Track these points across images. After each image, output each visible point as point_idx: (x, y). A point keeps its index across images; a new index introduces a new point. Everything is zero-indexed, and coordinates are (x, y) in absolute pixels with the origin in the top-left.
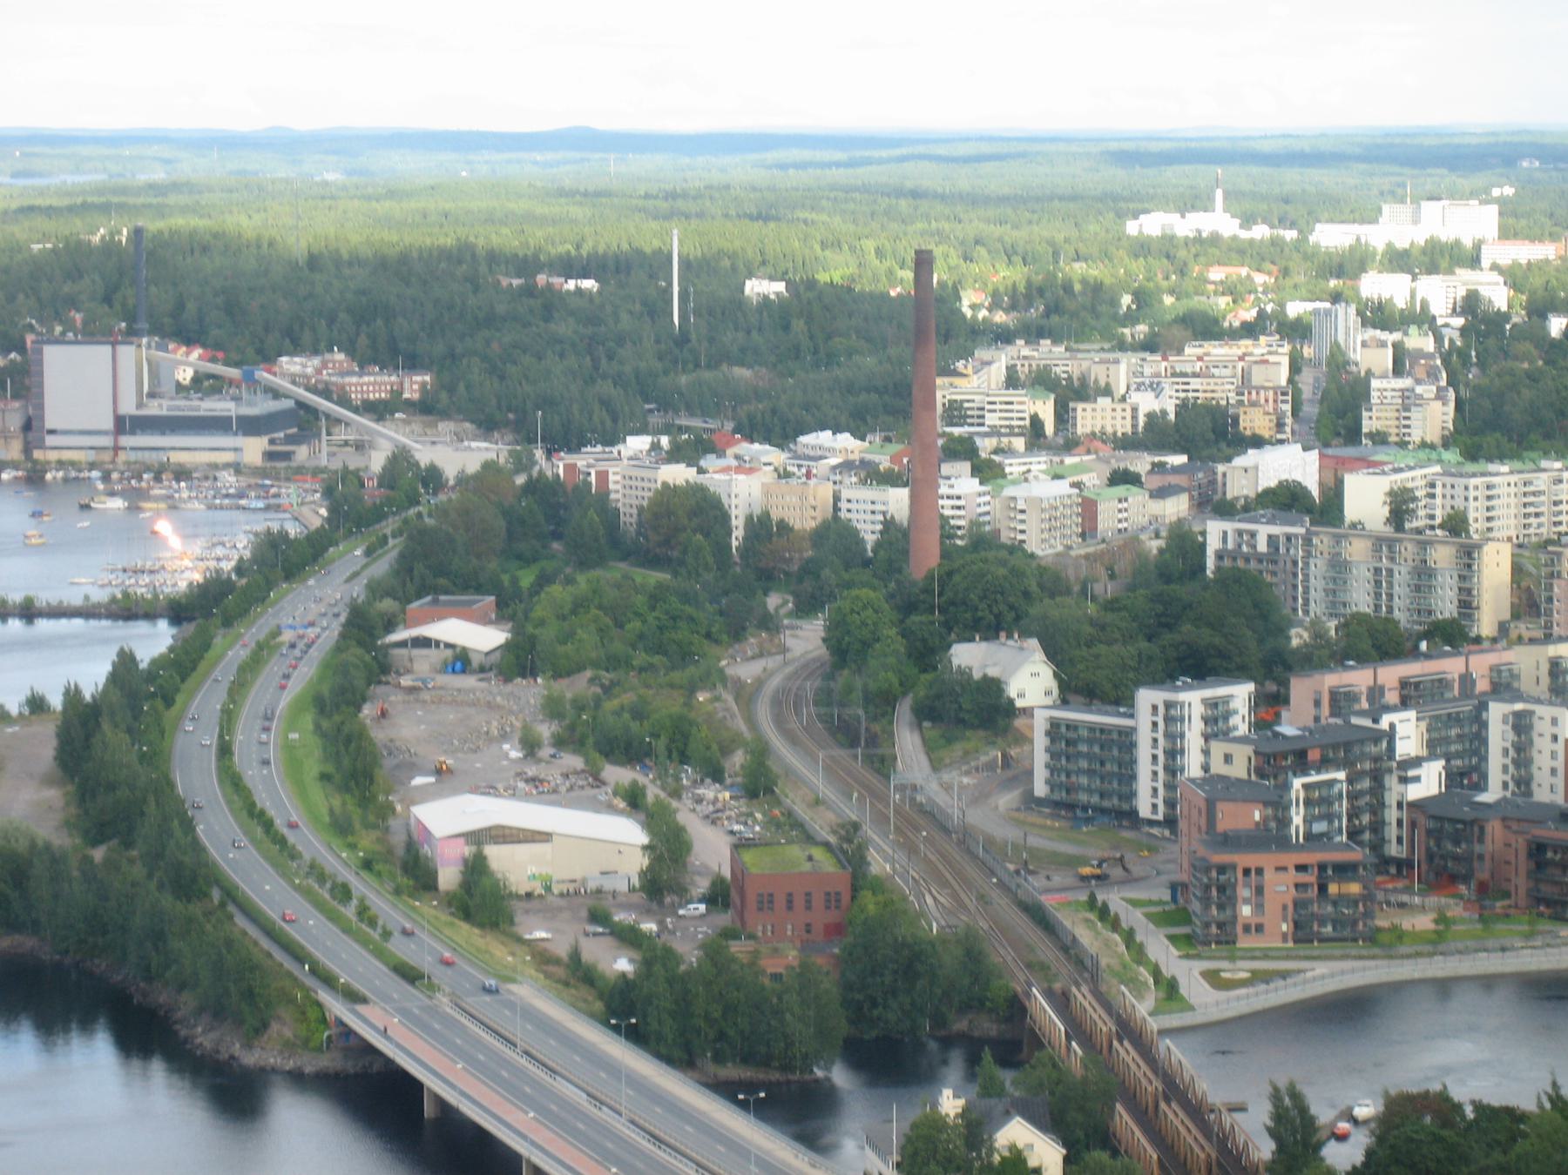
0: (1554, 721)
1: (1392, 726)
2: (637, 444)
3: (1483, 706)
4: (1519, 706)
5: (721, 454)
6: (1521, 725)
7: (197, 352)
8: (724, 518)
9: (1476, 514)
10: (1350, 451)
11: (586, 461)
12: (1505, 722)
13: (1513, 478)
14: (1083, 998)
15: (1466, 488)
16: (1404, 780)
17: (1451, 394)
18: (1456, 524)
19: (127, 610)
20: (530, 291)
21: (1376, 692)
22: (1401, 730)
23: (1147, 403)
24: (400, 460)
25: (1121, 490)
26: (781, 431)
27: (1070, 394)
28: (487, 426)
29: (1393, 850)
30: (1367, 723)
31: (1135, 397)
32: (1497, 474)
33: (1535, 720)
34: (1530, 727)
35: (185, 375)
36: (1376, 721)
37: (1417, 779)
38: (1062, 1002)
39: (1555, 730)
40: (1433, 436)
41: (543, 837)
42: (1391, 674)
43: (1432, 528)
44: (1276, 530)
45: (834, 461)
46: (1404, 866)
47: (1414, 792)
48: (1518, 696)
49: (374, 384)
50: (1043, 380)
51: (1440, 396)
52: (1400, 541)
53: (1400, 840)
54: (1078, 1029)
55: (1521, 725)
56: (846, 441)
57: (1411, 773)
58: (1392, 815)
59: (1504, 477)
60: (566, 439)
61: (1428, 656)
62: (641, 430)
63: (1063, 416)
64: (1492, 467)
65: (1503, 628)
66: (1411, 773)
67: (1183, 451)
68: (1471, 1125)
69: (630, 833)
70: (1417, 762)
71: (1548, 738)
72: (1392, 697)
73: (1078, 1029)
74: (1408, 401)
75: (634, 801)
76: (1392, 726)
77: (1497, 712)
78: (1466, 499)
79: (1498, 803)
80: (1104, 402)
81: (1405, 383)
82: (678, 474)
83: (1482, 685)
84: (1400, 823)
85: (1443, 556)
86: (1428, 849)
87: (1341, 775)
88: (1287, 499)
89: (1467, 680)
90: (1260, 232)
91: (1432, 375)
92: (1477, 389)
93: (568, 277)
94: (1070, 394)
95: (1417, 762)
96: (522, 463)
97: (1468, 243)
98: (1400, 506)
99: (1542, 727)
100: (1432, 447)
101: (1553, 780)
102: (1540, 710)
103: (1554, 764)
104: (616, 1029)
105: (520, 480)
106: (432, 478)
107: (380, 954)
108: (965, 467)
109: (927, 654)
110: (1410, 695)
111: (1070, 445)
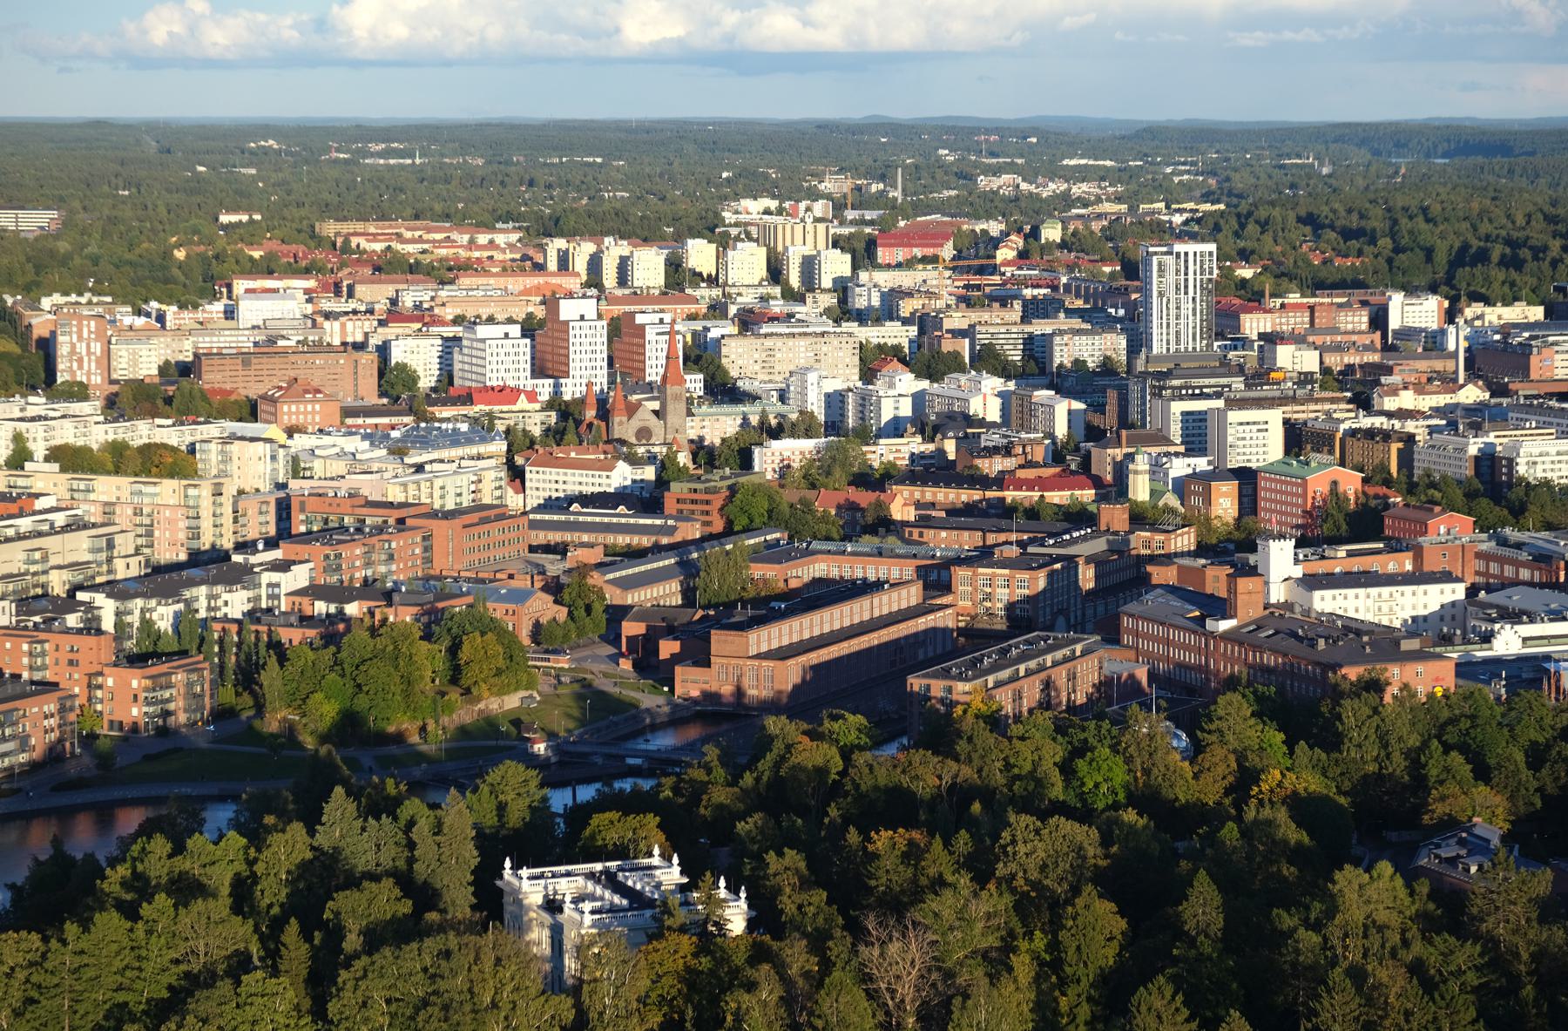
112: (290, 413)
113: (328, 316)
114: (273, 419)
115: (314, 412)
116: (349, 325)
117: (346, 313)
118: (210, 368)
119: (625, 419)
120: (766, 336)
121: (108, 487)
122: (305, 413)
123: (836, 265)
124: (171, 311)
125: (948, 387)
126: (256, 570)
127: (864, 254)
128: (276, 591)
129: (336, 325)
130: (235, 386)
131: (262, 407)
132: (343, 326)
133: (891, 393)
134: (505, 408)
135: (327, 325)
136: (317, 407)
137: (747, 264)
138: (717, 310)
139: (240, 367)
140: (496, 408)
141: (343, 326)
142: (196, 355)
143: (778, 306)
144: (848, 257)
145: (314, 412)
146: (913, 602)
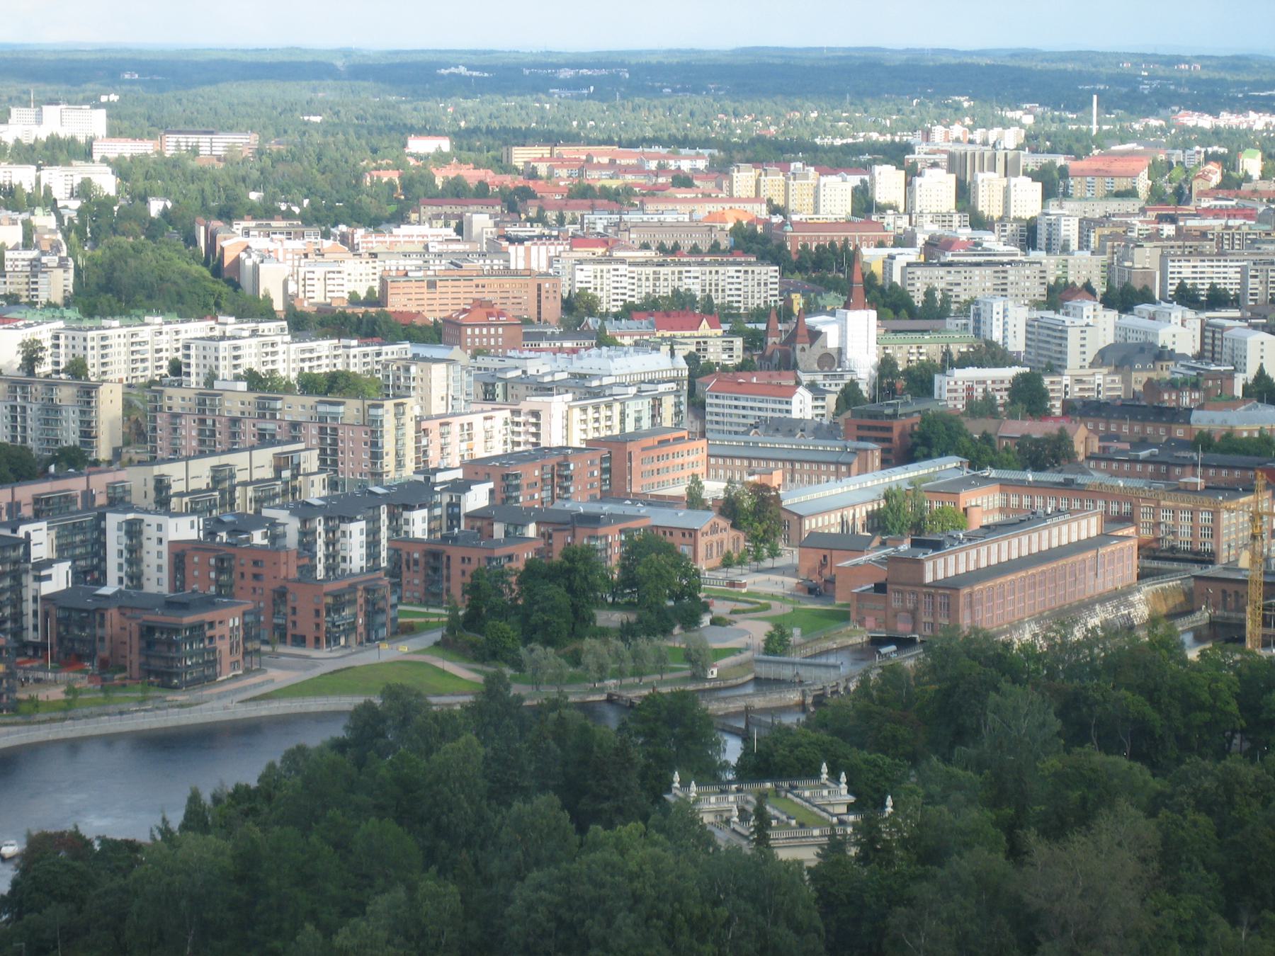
0: (160, 527)
1: (28, 535)
3: (102, 517)
4: (131, 516)
6: (133, 531)
9: (93, 360)
12: (119, 529)
13: (124, 331)
15: (85, 340)
16: (39, 579)
17: (71, 263)
18: (77, 369)
21: (14, 507)
22: (35, 538)
29: (30, 636)
30: (7, 532)
32: (109, 328)
33: (144, 527)
34: (140, 532)
36: (14, 531)
37: (49, 577)
39: (160, 534)
40: (57, 298)
42: (26, 493)
43: (57, 372)
46: (39, 648)
47: (47, 588)
48: (130, 508)
51: (62, 264)
52: (31, 383)
53: (35, 628)
55: (133, 531)
57: (44, 573)
58: (29, 607)
59: (116, 331)
61: (56, 477)
64: (105, 322)
65: (117, 453)
66: (44, 573)
68: (98, 856)
70: (49, 563)
71: (155, 541)
72: (27, 511)
74: (36, 267)
76: (28, 535)
77: (113, 521)
78: (85, 348)
79: (115, 594)
81: (33, 254)
83: (101, 500)
84: (35, 613)
85: (66, 395)
86: (59, 634)
89: (88, 496)
91: (55, 248)
92: (91, 259)
95: (49, 563)
97: (82, 139)
99: (150, 532)
100: (55, 306)
101: (159, 575)
102: (148, 518)
103: (160, 562)
110: (43, 508)
112: (473, 336)
113: (512, 240)
114: (457, 340)
115: (496, 336)
116: (534, 249)
117: (530, 238)
118: (396, 291)
119: (806, 346)
120: (950, 264)
122: (489, 336)
124: (360, 233)
125: (1136, 321)
126: (437, 489)
128: (456, 510)
129: (521, 249)
130: (420, 309)
131: (447, 330)
132: (528, 250)
133: (1078, 322)
134: (687, 333)
135: (512, 249)
136: (500, 330)
138: (904, 240)
139: (425, 290)
140: (678, 333)
141: (528, 250)
142: (383, 281)
143: (965, 233)
144: (1039, 185)
145: (496, 336)
146: (1093, 533)
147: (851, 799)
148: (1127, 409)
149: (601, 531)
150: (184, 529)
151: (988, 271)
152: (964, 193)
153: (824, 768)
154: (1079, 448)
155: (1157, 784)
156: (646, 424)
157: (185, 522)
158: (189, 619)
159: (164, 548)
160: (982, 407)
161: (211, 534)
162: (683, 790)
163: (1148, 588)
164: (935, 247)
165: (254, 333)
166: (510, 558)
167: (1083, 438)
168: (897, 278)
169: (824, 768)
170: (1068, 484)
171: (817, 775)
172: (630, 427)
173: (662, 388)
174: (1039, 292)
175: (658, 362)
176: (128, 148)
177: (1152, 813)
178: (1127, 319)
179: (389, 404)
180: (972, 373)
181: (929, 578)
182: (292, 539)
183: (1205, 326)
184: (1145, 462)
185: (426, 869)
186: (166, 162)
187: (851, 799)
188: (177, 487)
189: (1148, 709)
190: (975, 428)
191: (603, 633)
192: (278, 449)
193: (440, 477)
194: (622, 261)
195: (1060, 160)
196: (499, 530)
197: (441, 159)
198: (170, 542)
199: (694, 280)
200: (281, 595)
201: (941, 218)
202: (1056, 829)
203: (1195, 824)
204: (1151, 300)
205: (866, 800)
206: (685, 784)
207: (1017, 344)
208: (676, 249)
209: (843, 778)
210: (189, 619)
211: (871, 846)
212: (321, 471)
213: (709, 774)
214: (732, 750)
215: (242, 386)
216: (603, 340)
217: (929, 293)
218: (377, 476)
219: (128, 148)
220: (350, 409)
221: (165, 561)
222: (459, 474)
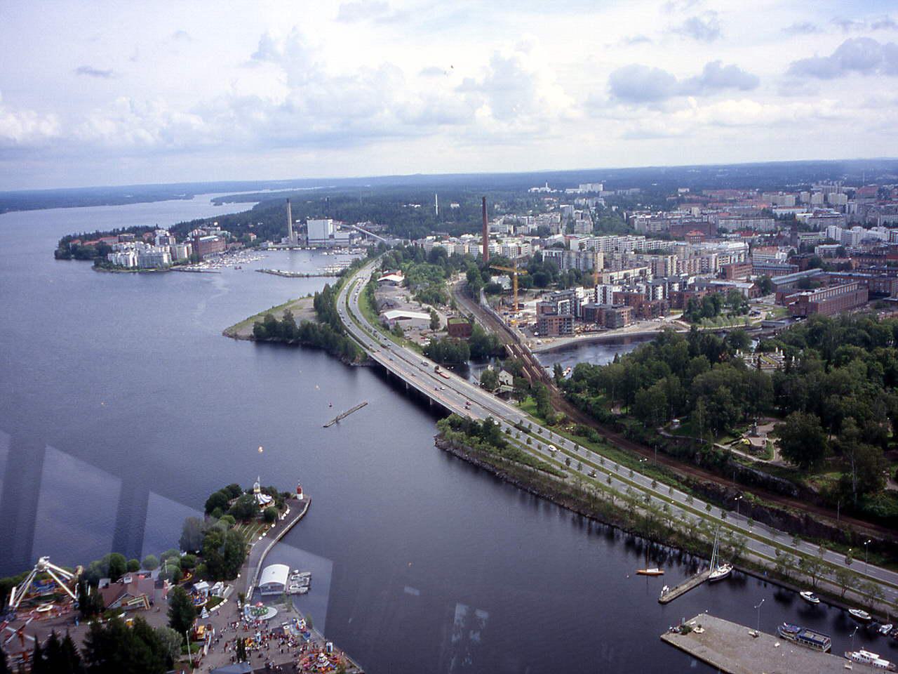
2: (429, 238)
5: (446, 240)
6: (605, 290)
7: (341, 223)
8: (446, 253)
10: (572, 235)
11: (419, 242)
14: (516, 346)
17: (592, 223)
18: (592, 249)
19: (328, 275)
20: (407, 208)
23: (531, 226)
24: (381, 244)
25: (525, 245)
26: (458, 235)
27: (517, 224)
28: (400, 236)
31: (529, 225)
35: (339, 227)
38: (513, 347)
41: (410, 318)
44: (556, 252)
45: (469, 240)
47: (583, 304)
49: (377, 227)
50: (510, 222)
54: (516, 352)
55: (605, 290)
56: (471, 236)
59: (602, 239)
60: (415, 238)
62: (431, 235)
63: (515, 230)
65: (602, 270)
67: (538, 236)
68: (592, 369)
69: (427, 317)
73: (516, 352)
75: (428, 311)
80: (523, 227)
82: (437, 244)
85: (590, 256)
87: (568, 300)
88: (558, 245)
90: (555, 191)
92: (598, 222)
93: (415, 204)
94: (517, 224)
96: (406, 243)
98: (581, 246)
104: (424, 356)
105: (406, 246)
106: (388, 247)
107: (379, 343)
108: (495, 241)
109: (486, 279)
111: (516, 236)
121: (648, 258)
123: (842, 199)
127: (850, 195)
137: (817, 198)
147: (783, 357)
148: (869, 255)
149: (723, 289)
150: (617, 289)
151: (832, 219)
152: (826, 198)
153: (777, 349)
154: (854, 266)
155: (868, 354)
156: (737, 261)
157: (617, 287)
158: (617, 311)
159: (612, 294)
160: (828, 255)
161: (623, 290)
162: (739, 354)
163: (871, 302)
164: (816, 213)
165: (637, 239)
166: (699, 296)
167: (855, 263)
168: (806, 221)
169: (777, 349)
170: (850, 275)
171: (775, 350)
172: (732, 262)
173: (741, 252)
174: (844, 224)
175: (741, 245)
176: (607, 193)
177: (865, 362)
178: (869, 231)
179: (670, 257)
180: (825, 246)
181: (810, 301)
182: (644, 291)
183: (891, 232)
184: (872, 269)
185: (672, 373)
186: (618, 197)
187: (783, 357)
188: (615, 278)
189: (867, 334)
190: (825, 261)
191: (722, 315)
192: (641, 269)
193: (682, 275)
194: (732, 219)
195: (853, 189)
196: (697, 289)
197: (686, 194)
198: (614, 293)
199: (751, 223)
200: (640, 306)
201: (819, 206)
202: (837, 365)
203: (877, 365)
204: (877, 226)
205: (788, 359)
206: (740, 353)
207: (839, 239)
208: (747, 216)
209: (782, 351)
210: (617, 311)
211: (788, 369)
212: (652, 274)
213: (748, 351)
214: (754, 344)
215: (633, 253)
216: (727, 239)
217: (815, 225)
218: (666, 276)
219: (607, 193)
220: (661, 257)
221: (612, 297)
222: (687, 274)
